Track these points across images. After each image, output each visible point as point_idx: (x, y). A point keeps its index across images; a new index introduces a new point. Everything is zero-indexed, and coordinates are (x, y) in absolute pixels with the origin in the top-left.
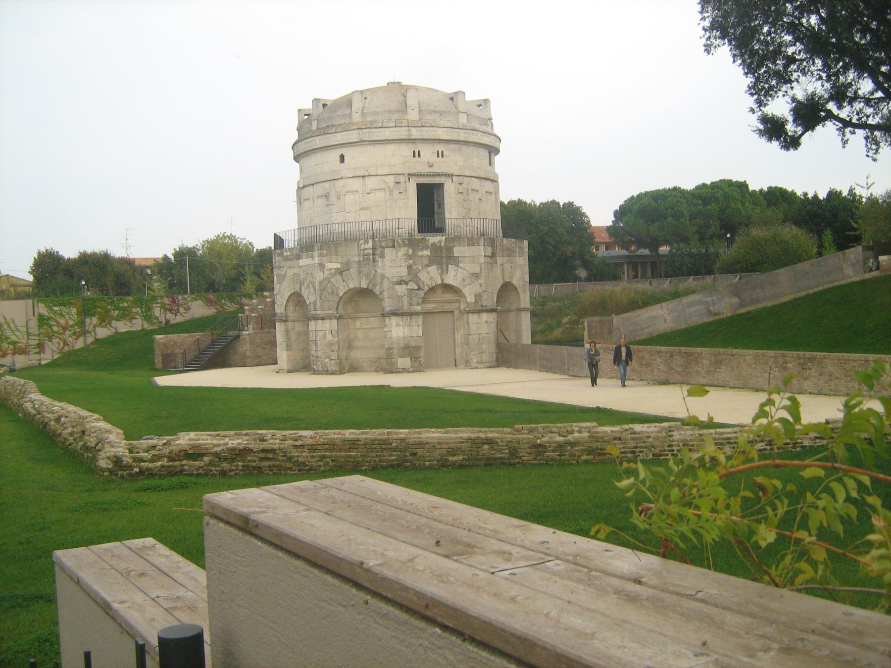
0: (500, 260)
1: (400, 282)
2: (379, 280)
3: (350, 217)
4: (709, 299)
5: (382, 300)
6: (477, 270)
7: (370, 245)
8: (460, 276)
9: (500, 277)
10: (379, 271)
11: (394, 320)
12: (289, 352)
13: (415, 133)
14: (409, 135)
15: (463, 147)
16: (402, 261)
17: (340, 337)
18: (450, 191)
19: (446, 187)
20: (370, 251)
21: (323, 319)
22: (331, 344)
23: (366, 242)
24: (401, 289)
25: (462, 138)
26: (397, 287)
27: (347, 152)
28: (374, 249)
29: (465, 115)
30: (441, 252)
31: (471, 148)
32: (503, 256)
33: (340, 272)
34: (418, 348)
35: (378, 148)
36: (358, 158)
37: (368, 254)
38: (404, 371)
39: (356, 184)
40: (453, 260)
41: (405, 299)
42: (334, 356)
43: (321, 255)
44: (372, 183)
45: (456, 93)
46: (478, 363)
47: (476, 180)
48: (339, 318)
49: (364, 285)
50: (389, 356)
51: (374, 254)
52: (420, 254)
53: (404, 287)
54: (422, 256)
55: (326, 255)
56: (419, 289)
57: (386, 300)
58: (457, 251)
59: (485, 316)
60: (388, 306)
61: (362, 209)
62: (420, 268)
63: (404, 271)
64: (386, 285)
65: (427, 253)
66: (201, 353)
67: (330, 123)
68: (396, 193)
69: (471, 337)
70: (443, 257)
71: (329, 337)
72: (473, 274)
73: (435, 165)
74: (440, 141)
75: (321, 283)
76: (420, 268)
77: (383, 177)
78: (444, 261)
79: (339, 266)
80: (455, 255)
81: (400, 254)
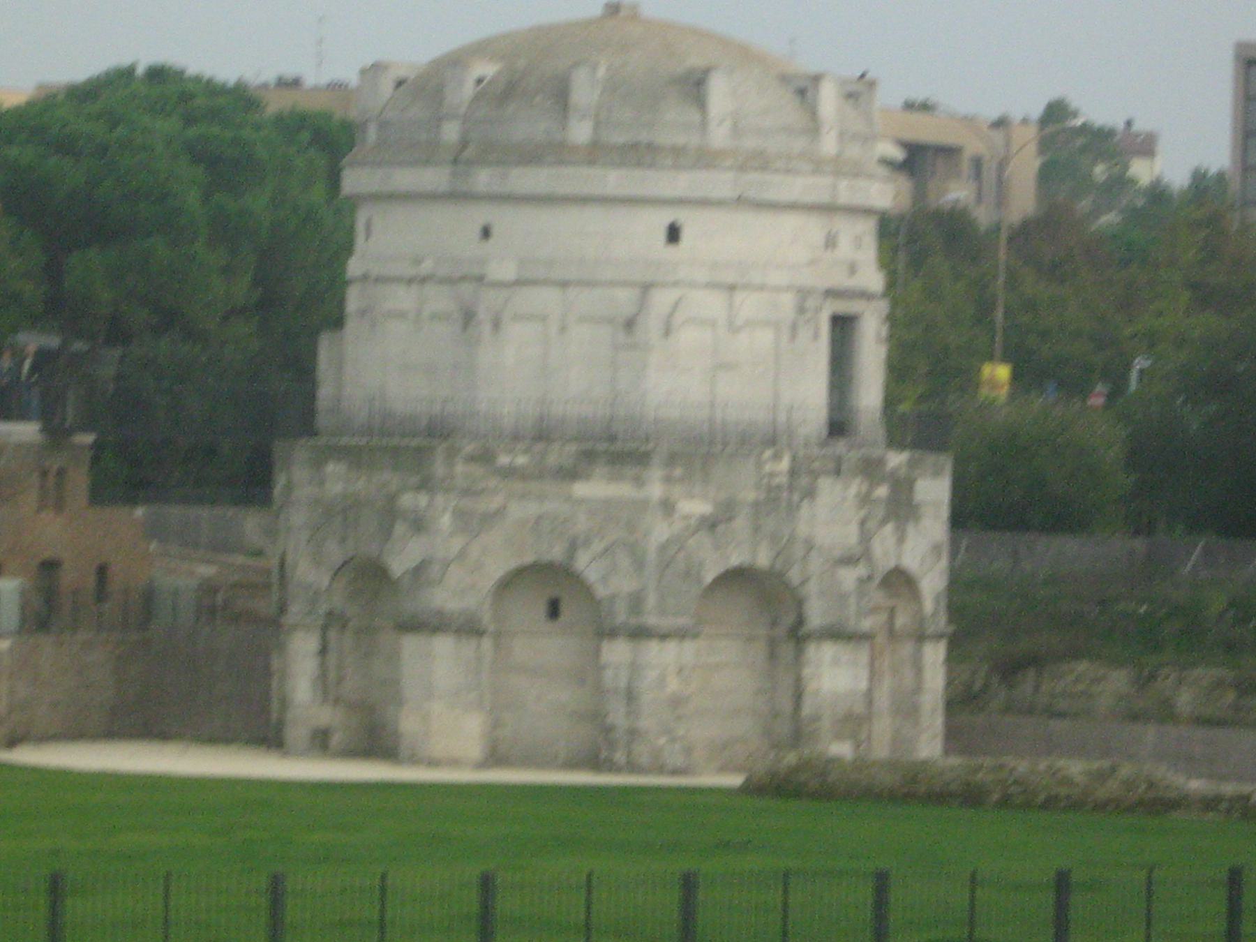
2: (799, 551)
7: (785, 464)
10: (803, 529)
21: (664, 637)
24: (849, 577)
28: (793, 473)
33: (710, 524)
36: (715, 239)
37: (779, 487)
43: (668, 480)
44: (749, 304)
49: (763, 559)
51: (791, 488)
64: (816, 564)
67: (644, 137)
75: (663, 548)
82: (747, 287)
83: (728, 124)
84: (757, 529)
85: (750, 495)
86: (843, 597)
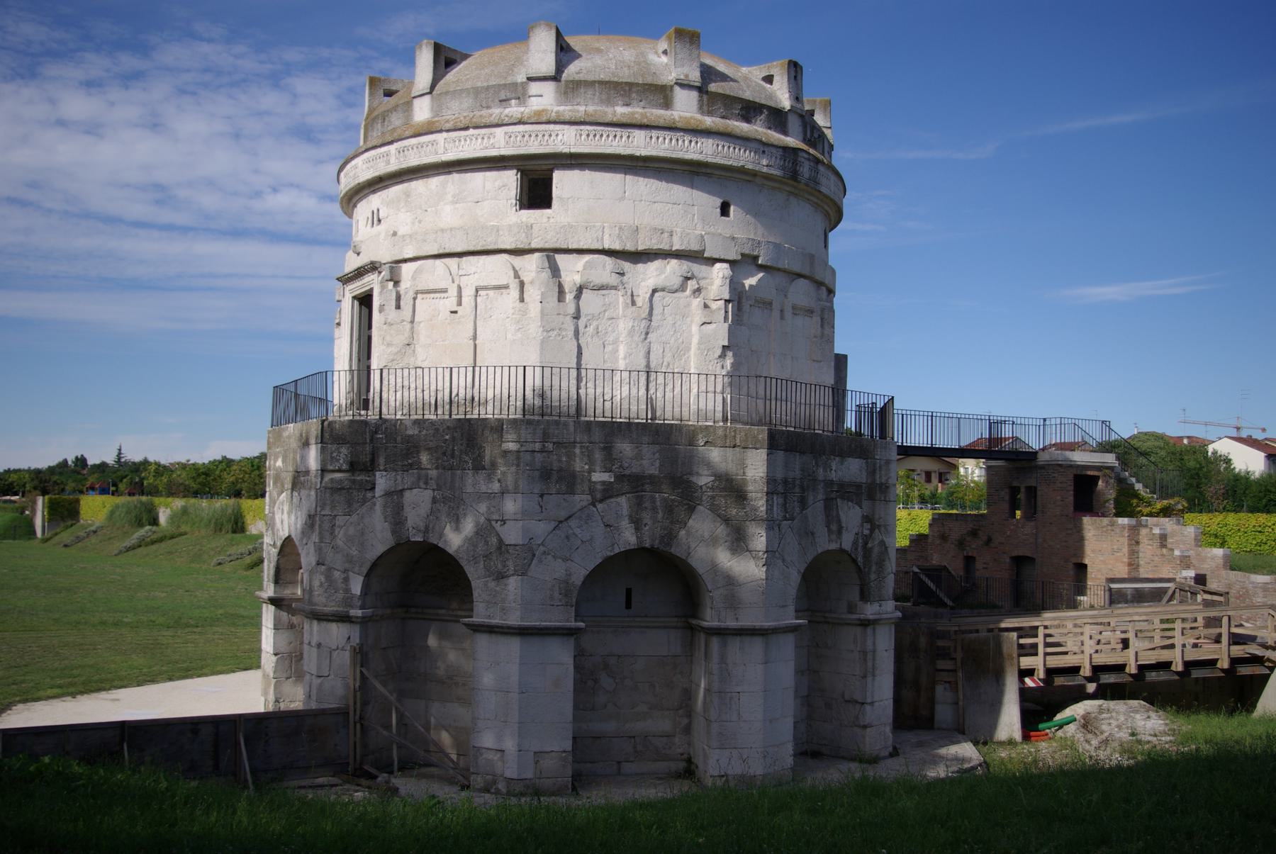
0: (382, 481)
15: (414, 184)
25: (394, 166)
31: (435, 182)
47: (438, 262)
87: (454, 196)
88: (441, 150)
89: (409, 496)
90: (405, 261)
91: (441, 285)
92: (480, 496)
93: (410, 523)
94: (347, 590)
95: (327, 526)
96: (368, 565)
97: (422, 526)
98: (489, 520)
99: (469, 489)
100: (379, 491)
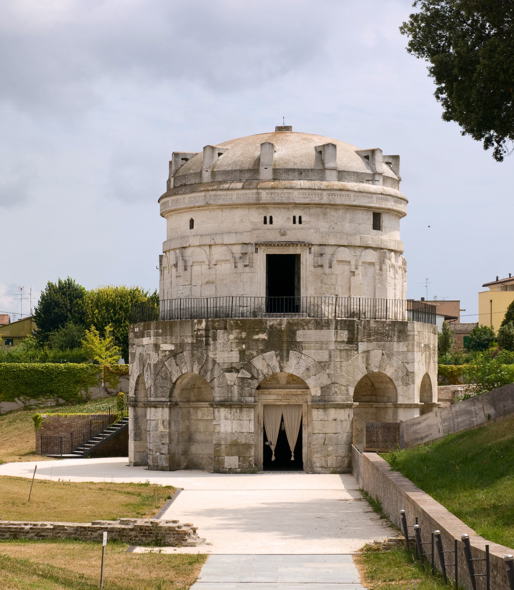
0: (362, 346)
1: (230, 370)
2: (210, 366)
3: (197, 292)
4: (472, 408)
5: (213, 388)
6: (324, 356)
8: (303, 364)
9: (362, 365)
10: (211, 355)
11: (223, 412)
12: (138, 443)
13: (265, 196)
14: (258, 199)
16: (234, 345)
17: (173, 428)
18: (307, 262)
19: (303, 259)
20: (203, 333)
21: (156, 407)
22: (162, 436)
23: (200, 322)
24: (231, 378)
26: (227, 374)
27: (199, 217)
28: (207, 330)
29: (335, 173)
30: (281, 336)
31: (340, 212)
32: (369, 341)
33: (174, 354)
34: (248, 446)
35: (227, 214)
37: (201, 336)
38: (231, 471)
39: (200, 254)
40: (293, 344)
41: (236, 389)
42: (165, 450)
43: (157, 335)
44: (218, 253)
45: (324, 146)
46: (322, 467)
47: (346, 249)
48: (173, 405)
50: (217, 454)
51: (207, 336)
52: (256, 337)
53: (235, 375)
54: (258, 340)
55: (161, 335)
56: (253, 378)
57: (216, 389)
58: (301, 335)
59: (333, 413)
60: (218, 395)
61: (207, 283)
62: (255, 353)
63: (234, 357)
65: (263, 336)
66: (91, 435)
67: (183, 182)
68: (240, 265)
69: (315, 437)
70: (284, 343)
71: (161, 428)
72: (320, 363)
73: (288, 232)
74: (296, 205)
75: (156, 365)
76: (255, 353)
77: (230, 247)
78: (285, 346)
79: (173, 348)
80: (298, 340)
81: (232, 337)
82: (216, 245)
83: (210, 170)
84: (193, 355)
85: (189, 340)
86: (229, 387)
87: (350, 219)
88: (352, 200)
89: (373, 353)
90: (326, 245)
91: (348, 259)
92: (399, 353)
93: (372, 365)
94: (348, 394)
95: (338, 366)
96: (356, 383)
97: (378, 365)
98: (403, 362)
99: (395, 350)
100: (360, 351)
